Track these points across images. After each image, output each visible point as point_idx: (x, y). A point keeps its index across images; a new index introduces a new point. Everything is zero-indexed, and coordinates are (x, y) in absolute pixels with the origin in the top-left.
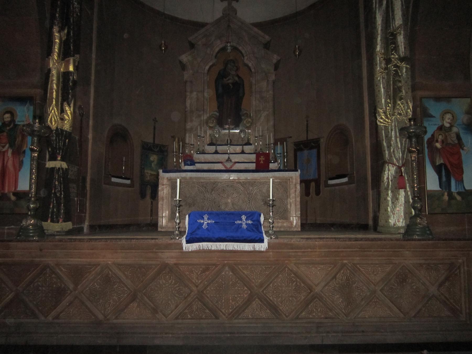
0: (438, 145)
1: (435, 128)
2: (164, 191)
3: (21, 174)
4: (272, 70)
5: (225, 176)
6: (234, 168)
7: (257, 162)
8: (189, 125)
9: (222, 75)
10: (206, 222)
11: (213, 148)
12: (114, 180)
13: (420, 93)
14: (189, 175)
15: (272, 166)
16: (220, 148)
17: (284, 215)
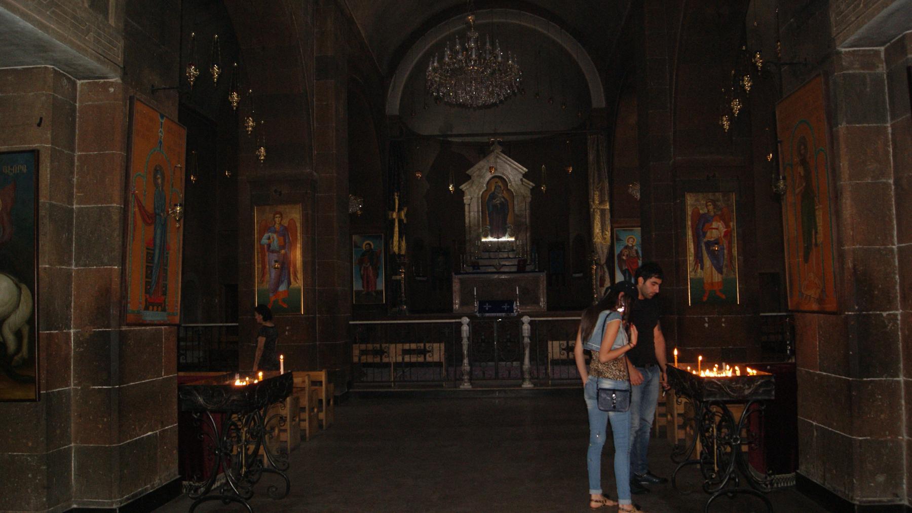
0: (624, 258)
1: (622, 247)
2: (456, 286)
3: (379, 280)
4: (529, 194)
5: (496, 276)
6: (502, 270)
7: (518, 265)
8: (468, 238)
9: (493, 196)
10: (487, 307)
11: (486, 255)
12: (419, 278)
13: (615, 225)
14: (472, 276)
15: (528, 268)
16: (492, 255)
17: (536, 301)
